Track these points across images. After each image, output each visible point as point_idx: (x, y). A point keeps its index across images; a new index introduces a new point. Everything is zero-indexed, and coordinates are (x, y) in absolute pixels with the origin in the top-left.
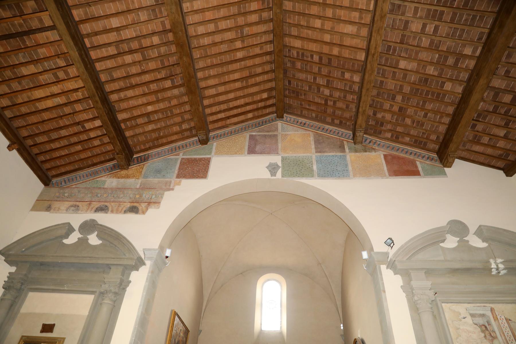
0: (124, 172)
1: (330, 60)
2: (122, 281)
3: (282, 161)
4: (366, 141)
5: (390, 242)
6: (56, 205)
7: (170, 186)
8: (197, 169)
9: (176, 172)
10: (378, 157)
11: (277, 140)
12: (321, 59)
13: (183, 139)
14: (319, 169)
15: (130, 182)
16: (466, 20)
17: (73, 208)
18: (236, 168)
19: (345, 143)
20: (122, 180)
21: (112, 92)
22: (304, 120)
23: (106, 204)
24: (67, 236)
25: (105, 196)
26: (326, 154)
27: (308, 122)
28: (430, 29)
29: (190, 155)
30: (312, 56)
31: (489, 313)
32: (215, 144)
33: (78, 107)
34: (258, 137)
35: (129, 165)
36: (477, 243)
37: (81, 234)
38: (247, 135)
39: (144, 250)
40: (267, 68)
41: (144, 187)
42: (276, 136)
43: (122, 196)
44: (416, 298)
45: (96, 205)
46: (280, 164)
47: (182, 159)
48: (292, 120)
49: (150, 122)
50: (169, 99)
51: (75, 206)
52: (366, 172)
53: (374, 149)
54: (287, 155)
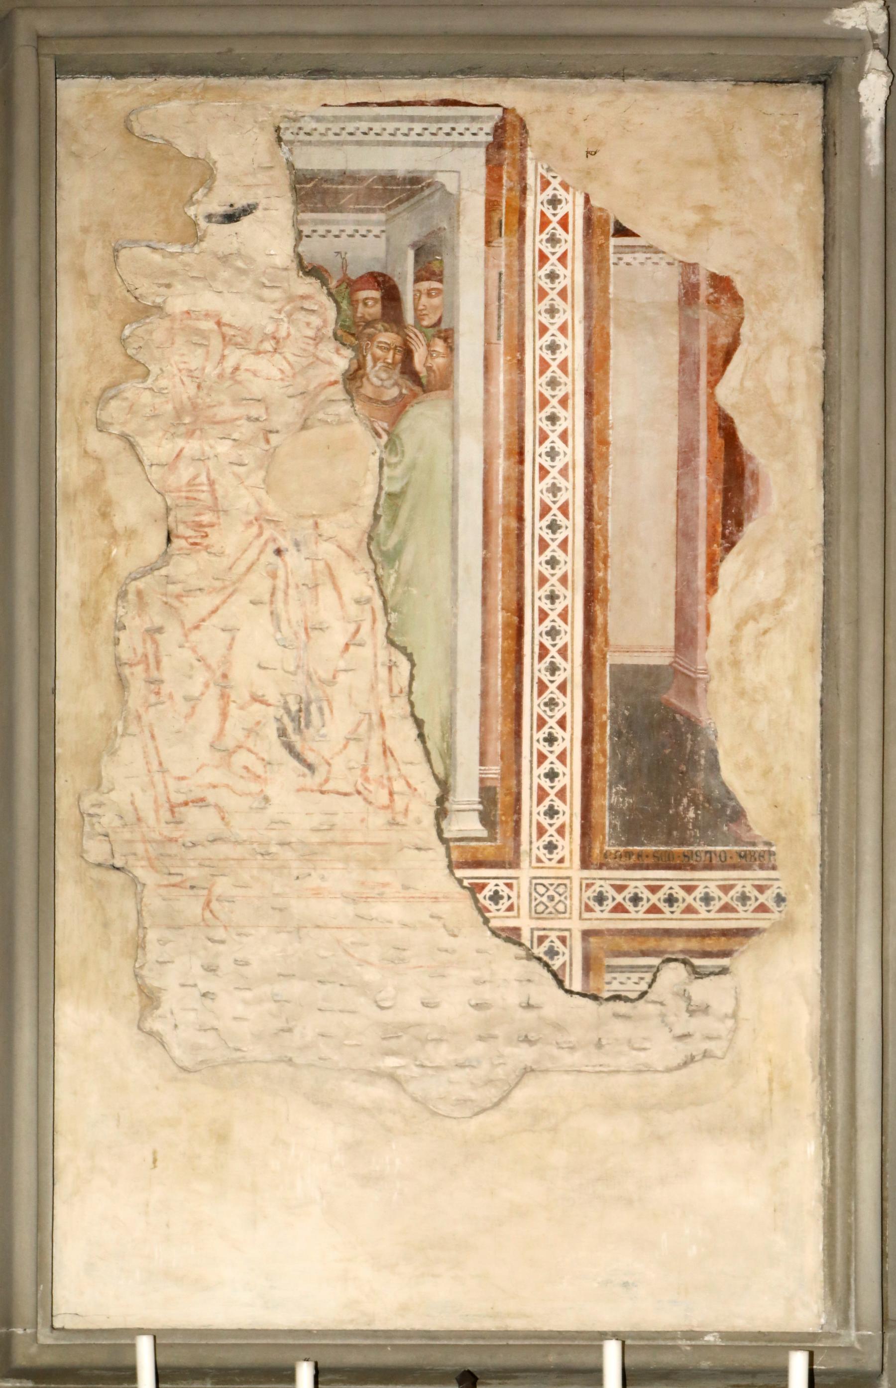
31: (464, 174)
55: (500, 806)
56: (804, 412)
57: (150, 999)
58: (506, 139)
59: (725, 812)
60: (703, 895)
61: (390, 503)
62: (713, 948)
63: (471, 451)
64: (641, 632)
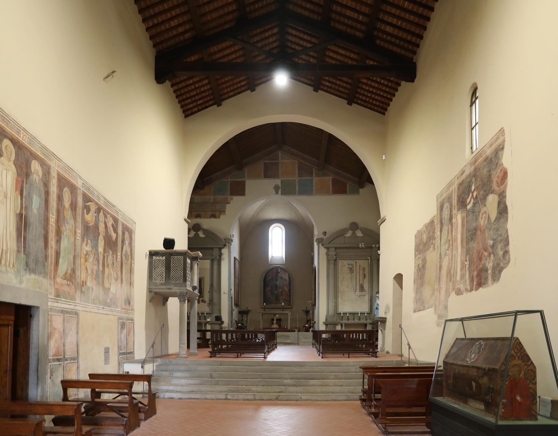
32: (246, 170)
36: (359, 234)
42: (277, 164)
46: (280, 186)
52: (321, 191)
58: (356, 262)
60: (364, 293)
64: (361, 282)
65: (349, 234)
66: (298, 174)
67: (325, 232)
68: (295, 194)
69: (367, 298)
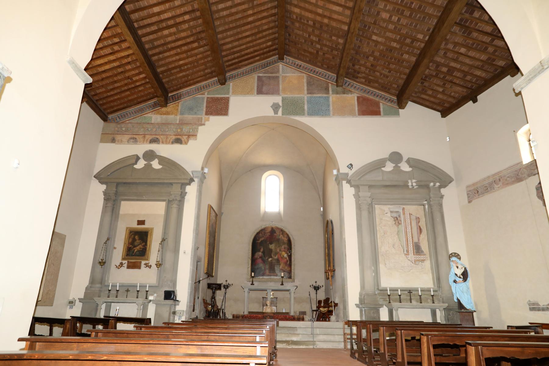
0: (164, 109)
1: (321, 27)
2: (182, 192)
3: (283, 101)
4: (345, 83)
5: (351, 166)
6: (118, 137)
7: (201, 121)
8: (219, 107)
9: (205, 110)
10: (352, 98)
11: (279, 82)
12: (314, 24)
13: (206, 80)
14: (309, 108)
15: (171, 117)
16: (420, 17)
17: (132, 140)
18: (248, 106)
19: (330, 85)
20: (164, 116)
21: (154, 55)
22: (298, 62)
23: (156, 136)
24: (136, 163)
25: (154, 130)
26: (315, 95)
27: (303, 64)
28: (395, 18)
29: (213, 94)
30: (308, 21)
31: (401, 211)
32: (231, 84)
33: (129, 67)
34: (264, 79)
35: (167, 103)
36: (405, 167)
37: (145, 160)
38: (255, 76)
39: (192, 172)
40: (272, 25)
41: (182, 123)
43: (167, 130)
44: (360, 202)
45: (149, 137)
46: (281, 104)
47: (208, 98)
48: (291, 62)
49: (181, 71)
50: (196, 55)
51: (133, 138)
52: (342, 111)
53: (351, 91)
54: (286, 96)
55: (408, 251)
56: (425, 225)
57: (385, 264)
58: (403, 209)
59: (422, 252)
60: (422, 257)
61: (398, 231)
62: (423, 261)
63: (403, 228)
64: (416, 240)
65: (389, 167)
66: (308, 90)
67: (351, 165)
68: (304, 115)
69: (427, 264)
